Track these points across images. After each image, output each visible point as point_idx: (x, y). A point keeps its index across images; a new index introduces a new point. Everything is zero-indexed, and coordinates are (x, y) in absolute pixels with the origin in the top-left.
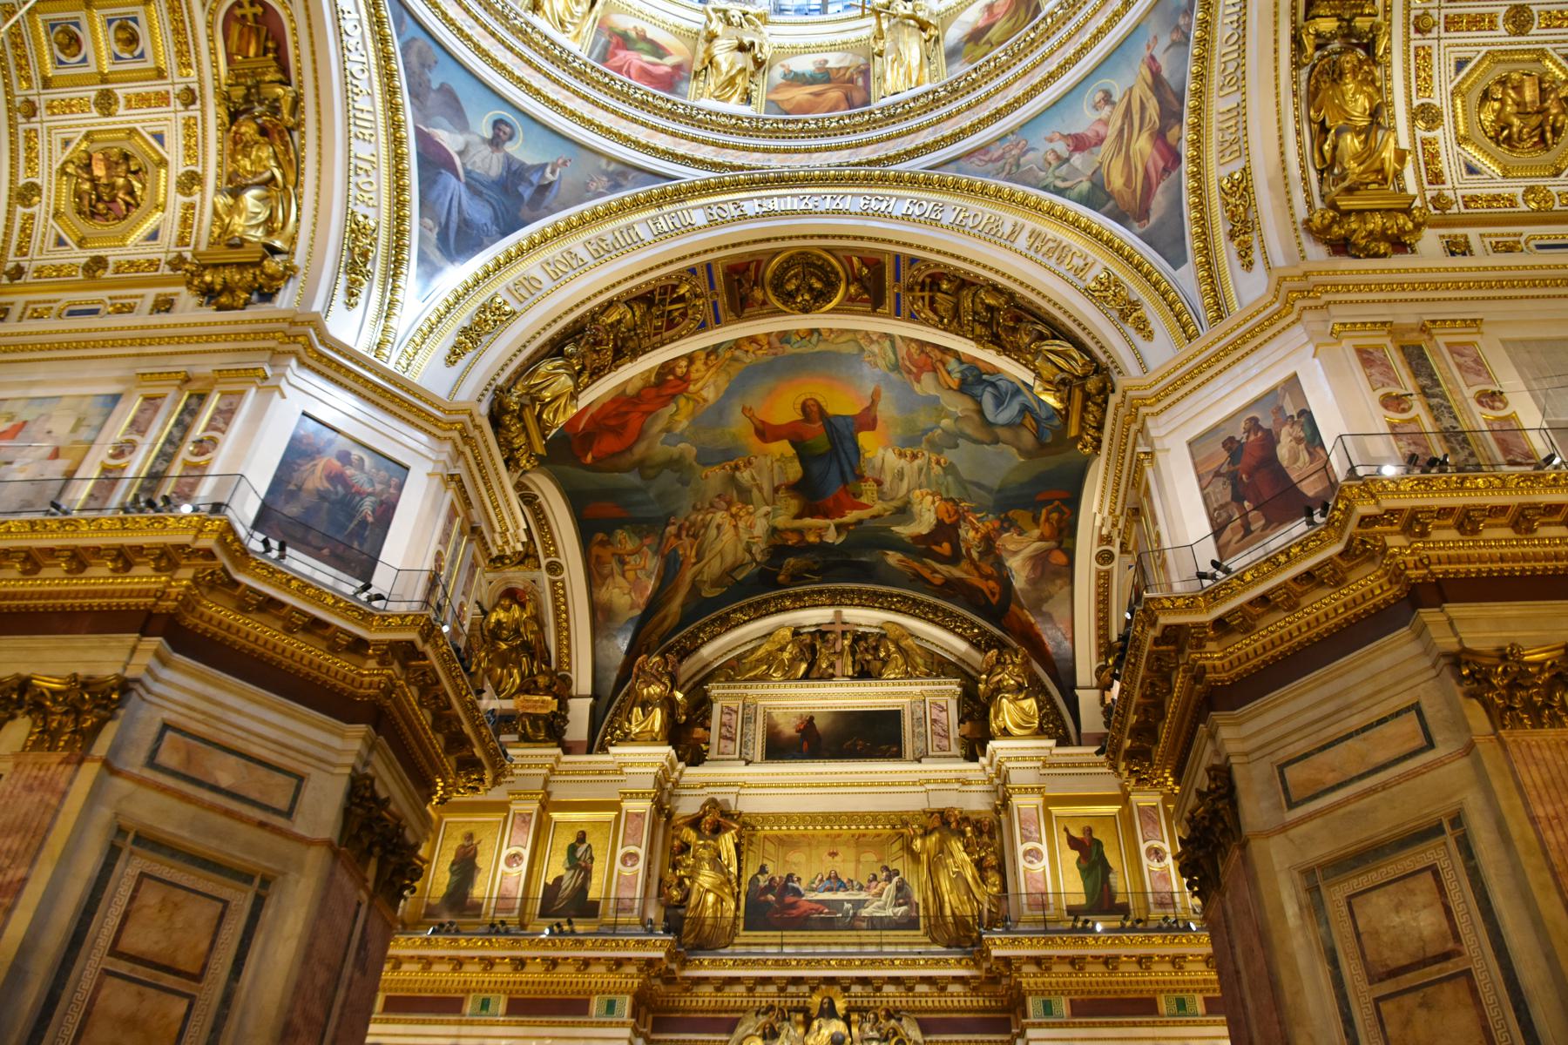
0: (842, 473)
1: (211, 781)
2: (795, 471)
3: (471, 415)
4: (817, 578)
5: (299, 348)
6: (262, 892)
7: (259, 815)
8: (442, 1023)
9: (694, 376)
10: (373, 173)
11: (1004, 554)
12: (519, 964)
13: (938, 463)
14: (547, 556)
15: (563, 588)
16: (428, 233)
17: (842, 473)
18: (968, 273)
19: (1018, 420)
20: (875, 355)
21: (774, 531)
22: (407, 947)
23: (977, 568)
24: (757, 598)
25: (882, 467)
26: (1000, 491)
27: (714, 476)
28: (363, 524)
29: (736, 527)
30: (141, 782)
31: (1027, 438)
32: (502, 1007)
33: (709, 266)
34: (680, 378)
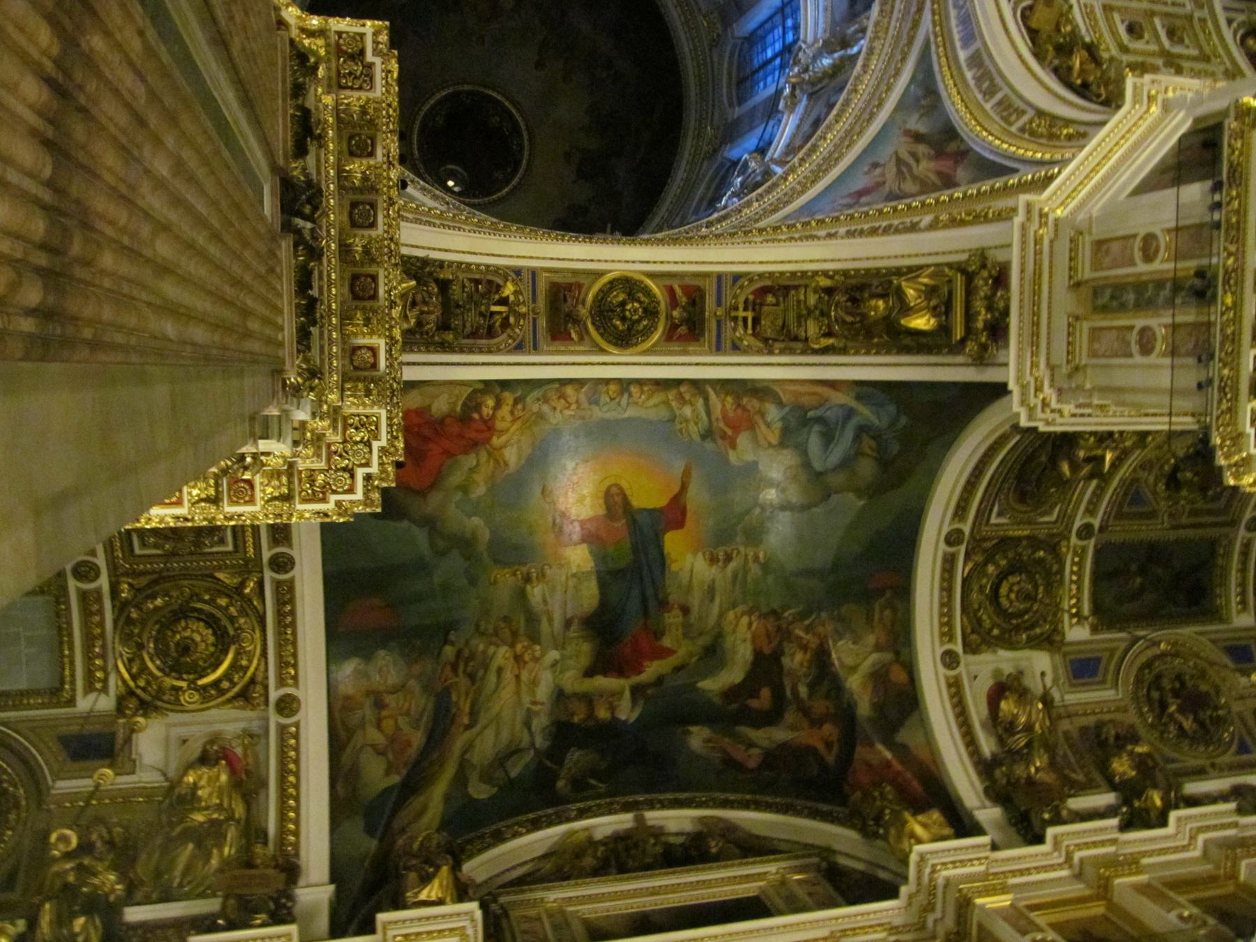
0: (644, 600)
2: (589, 595)
4: (602, 787)
9: (499, 425)
11: (842, 673)
13: (756, 559)
14: (281, 682)
15: (296, 736)
17: (644, 600)
18: (793, 274)
19: (852, 452)
20: (687, 421)
21: (560, 696)
23: (805, 711)
24: (531, 816)
25: (690, 587)
26: (835, 568)
27: (505, 580)
31: (867, 469)
33: (534, 273)
34: (485, 422)
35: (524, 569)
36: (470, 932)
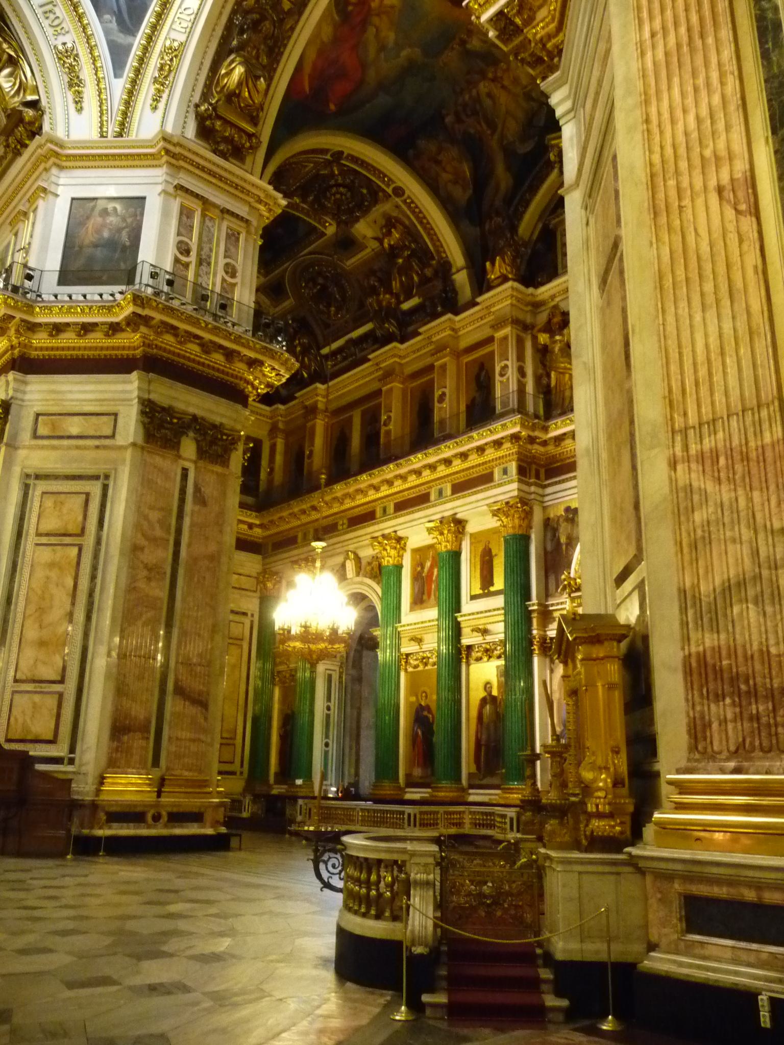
1: (68, 434)
3: (164, 139)
5: (53, 160)
6: (106, 482)
7: (97, 442)
8: (419, 510)
10: (56, 10)
12: (448, 462)
14: (388, 186)
16: (110, 25)
22: (389, 472)
27: (451, 58)
28: (124, 249)
29: (503, 87)
30: (31, 448)
32: (449, 492)
35: (457, 40)
36: (515, 294)
